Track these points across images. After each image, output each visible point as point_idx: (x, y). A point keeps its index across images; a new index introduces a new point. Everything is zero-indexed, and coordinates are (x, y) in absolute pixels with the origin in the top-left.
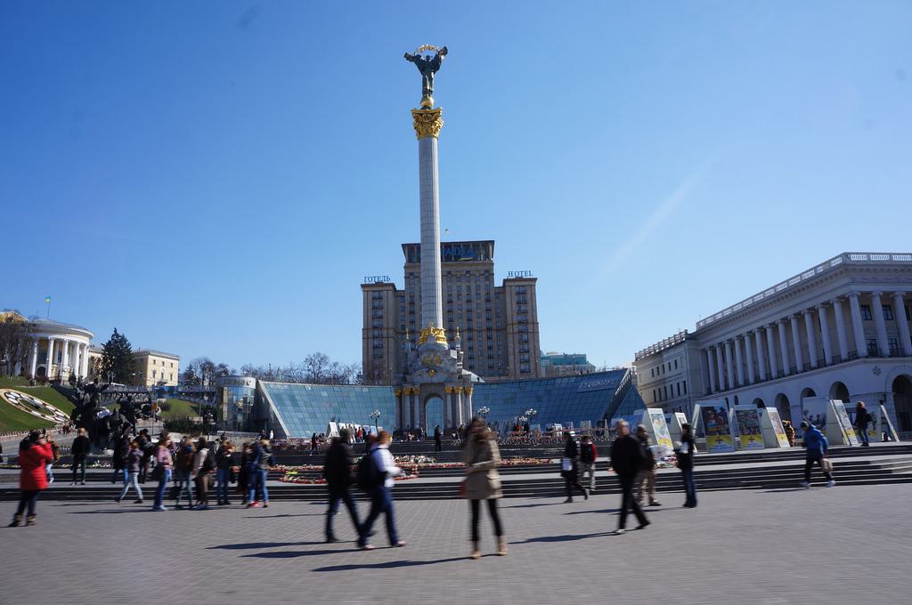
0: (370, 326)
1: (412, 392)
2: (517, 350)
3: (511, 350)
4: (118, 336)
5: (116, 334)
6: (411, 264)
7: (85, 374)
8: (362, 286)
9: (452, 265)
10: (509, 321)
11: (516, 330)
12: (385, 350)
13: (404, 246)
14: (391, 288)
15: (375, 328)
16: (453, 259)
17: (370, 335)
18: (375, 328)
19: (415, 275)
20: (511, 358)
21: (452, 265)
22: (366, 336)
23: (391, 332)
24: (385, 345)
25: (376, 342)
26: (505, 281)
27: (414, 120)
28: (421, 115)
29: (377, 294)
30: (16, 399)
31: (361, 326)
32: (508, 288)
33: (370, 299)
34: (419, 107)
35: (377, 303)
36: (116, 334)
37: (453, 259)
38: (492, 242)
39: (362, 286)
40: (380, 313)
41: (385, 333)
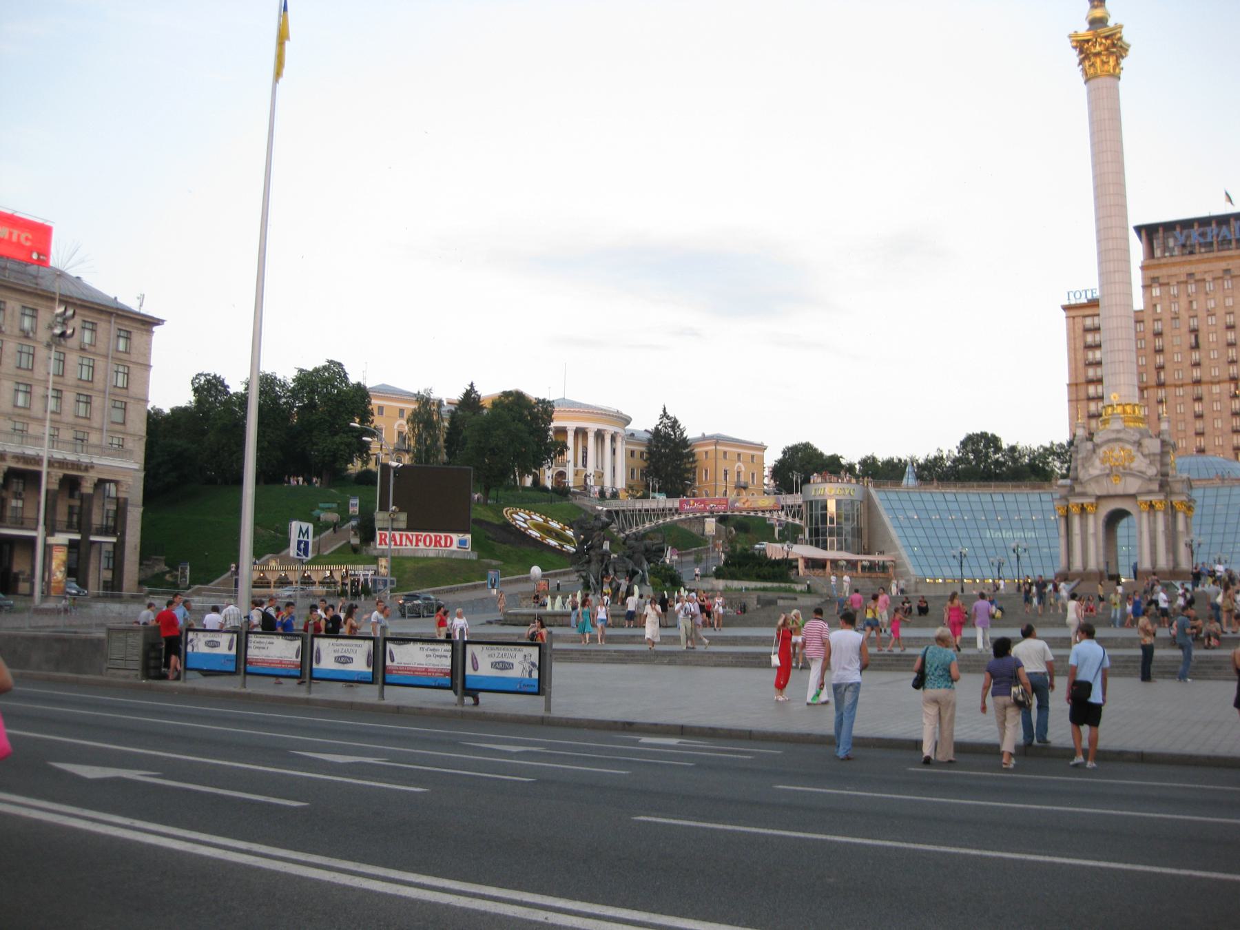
0: (1082, 379)
1: (1083, 509)
4: (668, 417)
5: (665, 415)
6: (1155, 262)
7: (621, 484)
8: (1066, 308)
9: (1230, 257)
15: (1090, 382)
16: (1234, 243)
17: (1082, 395)
18: (1090, 382)
19: (1161, 281)
21: (1230, 257)
22: (1074, 397)
27: (1074, 57)
28: (1088, 41)
29: (1089, 322)
30: (525, 522)
31: (1065, 379)
33: (1079, 331)
34: (1083, 28)
35: (1090, 338)
36: (665, 415)
37: (1234, 243)
39: (1066, 308)
40: (1098, 355)
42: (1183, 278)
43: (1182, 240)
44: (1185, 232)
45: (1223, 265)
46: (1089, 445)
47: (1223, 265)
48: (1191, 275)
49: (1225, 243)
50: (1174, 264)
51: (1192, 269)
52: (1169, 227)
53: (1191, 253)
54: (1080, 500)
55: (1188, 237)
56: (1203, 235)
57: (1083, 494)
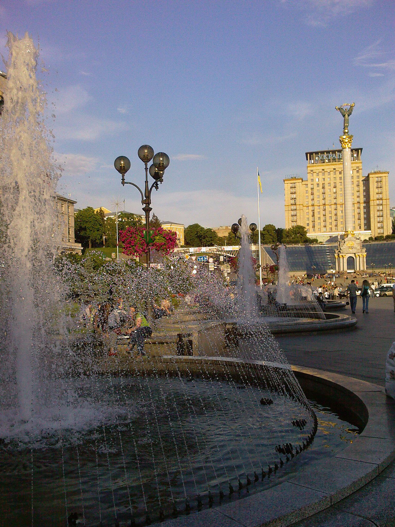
2: (376, 215)
3: (372, 215)
10: (372, 198)
11: (375, 204)
12: (298, 217)
13: (307, 154)
14: (301, 181)
19: (314, 171)
20: (372, 220)
21: (336, 164)
23: (301, 206)
24: (298, 215)
25: (293, 213)
26: (369, 175)
29: (293, 185)
32: (371, 179)
38: (361, 149)
41: (298, 206)
42: (321, 171)
43: (321, 158)
44: (322, 155)
45: (334, 167)
46: (343, 241)
47: (334, 167)
48: (323, 170)
49: (334, 160)
50: (318, 166)
51: (323, 168)
52: (317, 153)
53: (324, 162)
54: (342, 254)
55: (323, 157)
56: (328, 156)
57: (342, 253)
